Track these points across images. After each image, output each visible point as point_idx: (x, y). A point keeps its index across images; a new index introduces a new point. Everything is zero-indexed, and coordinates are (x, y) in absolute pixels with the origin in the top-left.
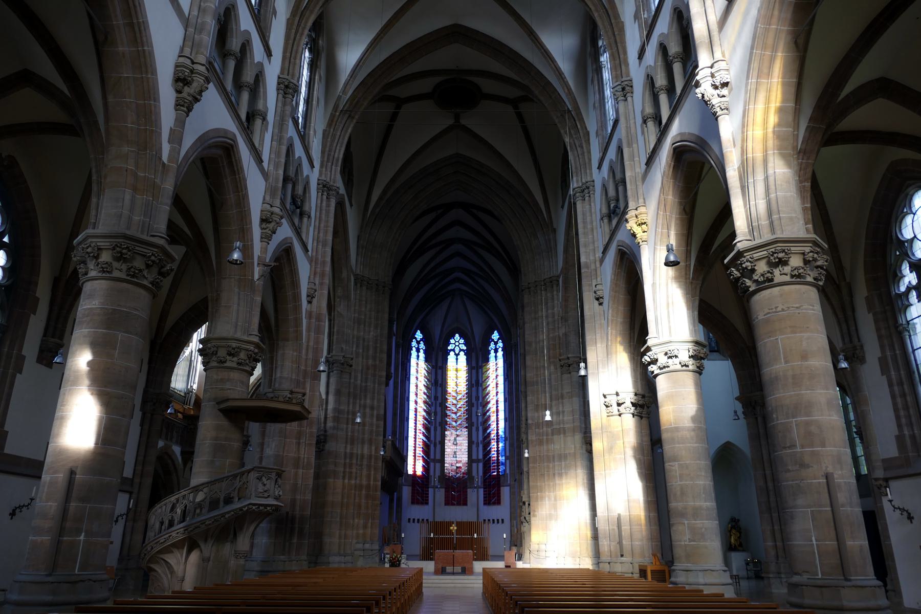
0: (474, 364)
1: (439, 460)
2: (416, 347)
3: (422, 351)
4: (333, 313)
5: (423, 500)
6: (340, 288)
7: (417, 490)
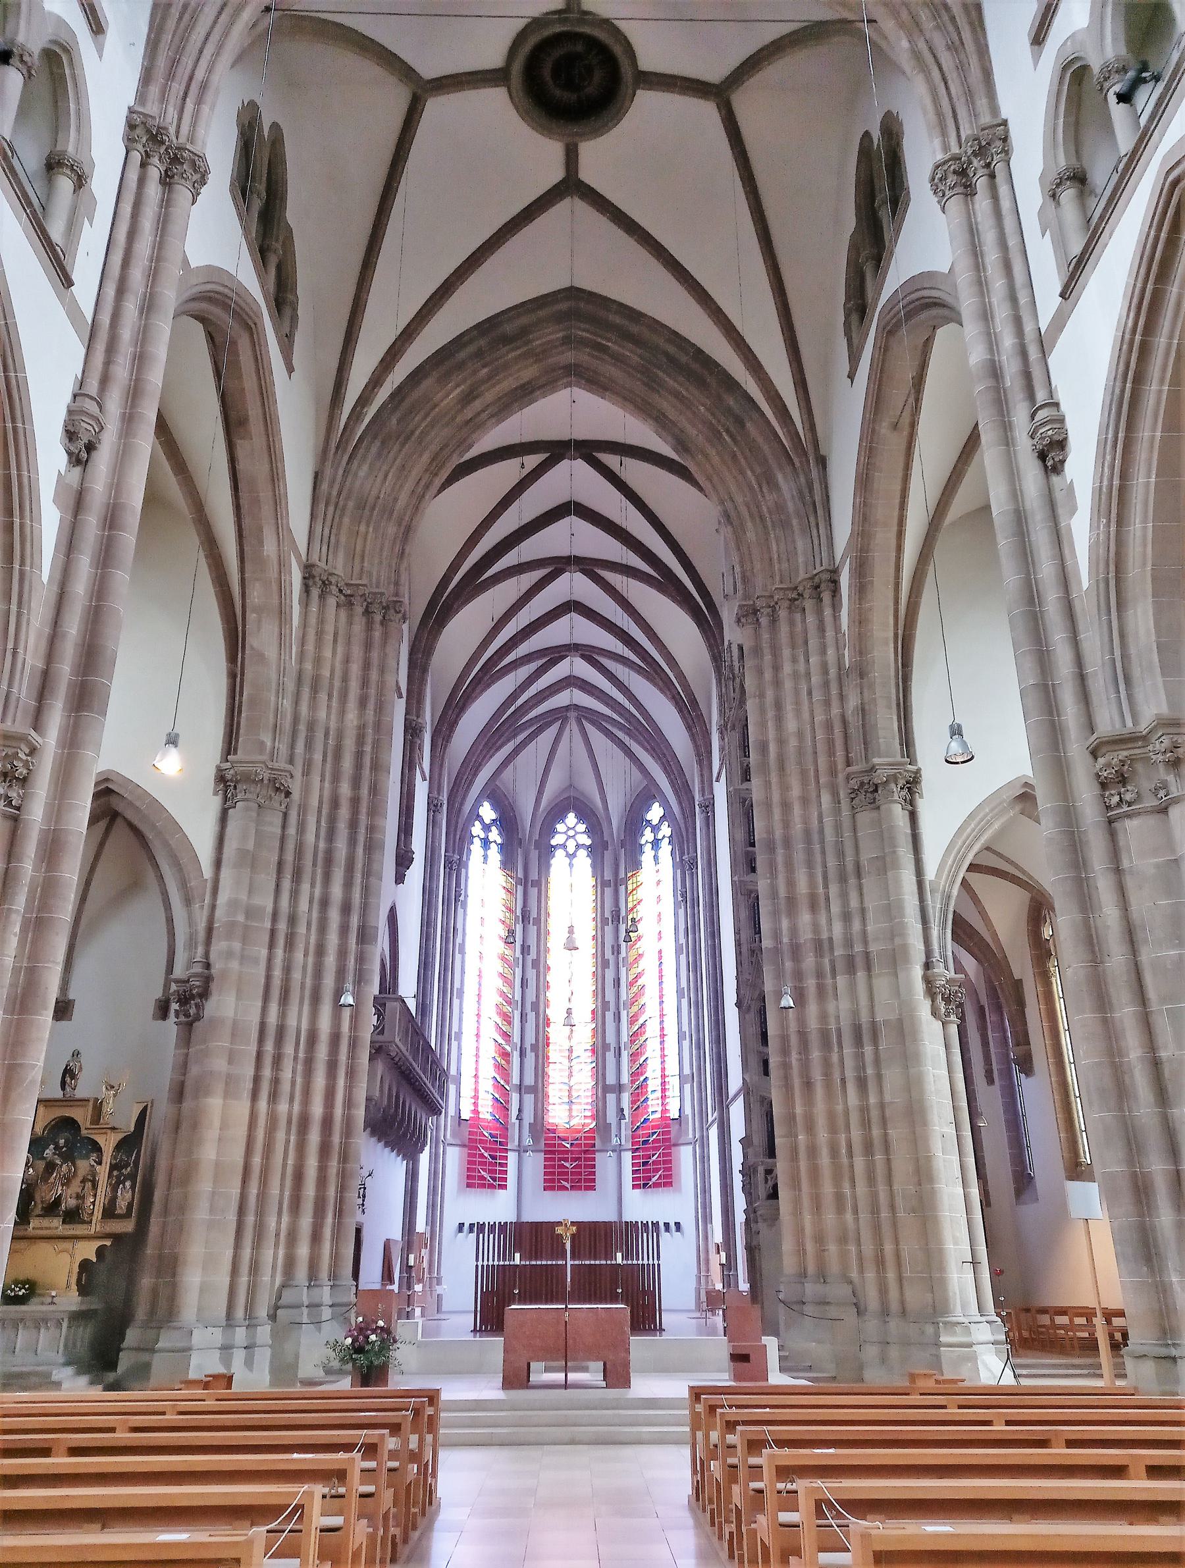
0: (608, 876)
1: (530, 1086)
2: (482, 835)
3: (493, 846)
4: (240, 655)
5: (494, 1179)
6: (257, 584)
7: (482, 1156)
